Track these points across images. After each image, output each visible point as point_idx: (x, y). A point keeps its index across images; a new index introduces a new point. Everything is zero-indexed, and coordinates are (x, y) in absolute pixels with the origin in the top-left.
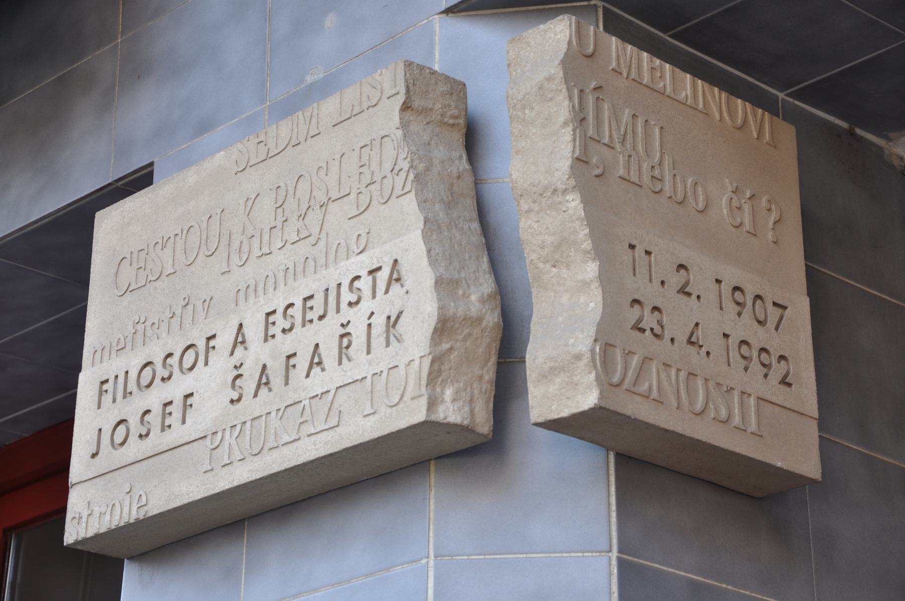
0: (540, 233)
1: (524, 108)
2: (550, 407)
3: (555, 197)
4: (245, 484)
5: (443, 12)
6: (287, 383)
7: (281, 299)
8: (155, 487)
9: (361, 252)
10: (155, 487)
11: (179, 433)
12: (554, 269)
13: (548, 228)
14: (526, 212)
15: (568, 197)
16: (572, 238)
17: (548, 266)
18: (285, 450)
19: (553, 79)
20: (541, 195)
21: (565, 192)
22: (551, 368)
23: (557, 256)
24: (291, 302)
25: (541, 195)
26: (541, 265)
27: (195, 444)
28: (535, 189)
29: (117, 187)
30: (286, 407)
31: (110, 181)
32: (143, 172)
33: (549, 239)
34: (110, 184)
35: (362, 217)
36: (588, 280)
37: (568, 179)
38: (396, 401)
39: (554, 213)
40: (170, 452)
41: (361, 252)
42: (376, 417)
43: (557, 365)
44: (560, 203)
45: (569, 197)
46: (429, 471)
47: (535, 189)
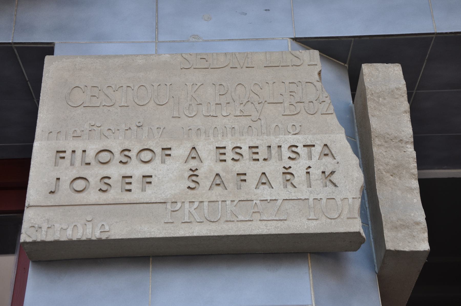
0: (387, 158)
1: (379, 97)
2: (398, 244)
3: (400, 144)
4: (202, 237)
5: (292, 38)
6: (336, 186)
7: (230, 142)
8: (117, 222)
9: (295, 134)
10: (117, 222)
11: (136, 195)
12: (391, 177)
13: (392, 156)
14: (378, 145)
15: (408, 146)
16: (407, 165)
17: (388, 175)
18: (240, 224)
19: (400, 90)
20: (391, 140)
21: (407, 143)
22: (401, 225)
23: (395, 172)
24: (241, 146)
25: (391, 140)
26: (384, 173)
27: (154, 205)
28: (388, 136)
29: (12, 47)
30: (239, 201)
31: (11, 42)
32: (39, 46)
33: (392, 162)
34: (10, 43)
35: (293, 116)
36: (413, 188)
37: (410, 137)
38: (336, 217)
39: (398, 151)
40: (129, 205)
41: (295, 134)
42: (318, 222)
43: (405, 224)
44: (403, 147)
45: (409, 146)
46: (149, 266)
47: (388, 136)
